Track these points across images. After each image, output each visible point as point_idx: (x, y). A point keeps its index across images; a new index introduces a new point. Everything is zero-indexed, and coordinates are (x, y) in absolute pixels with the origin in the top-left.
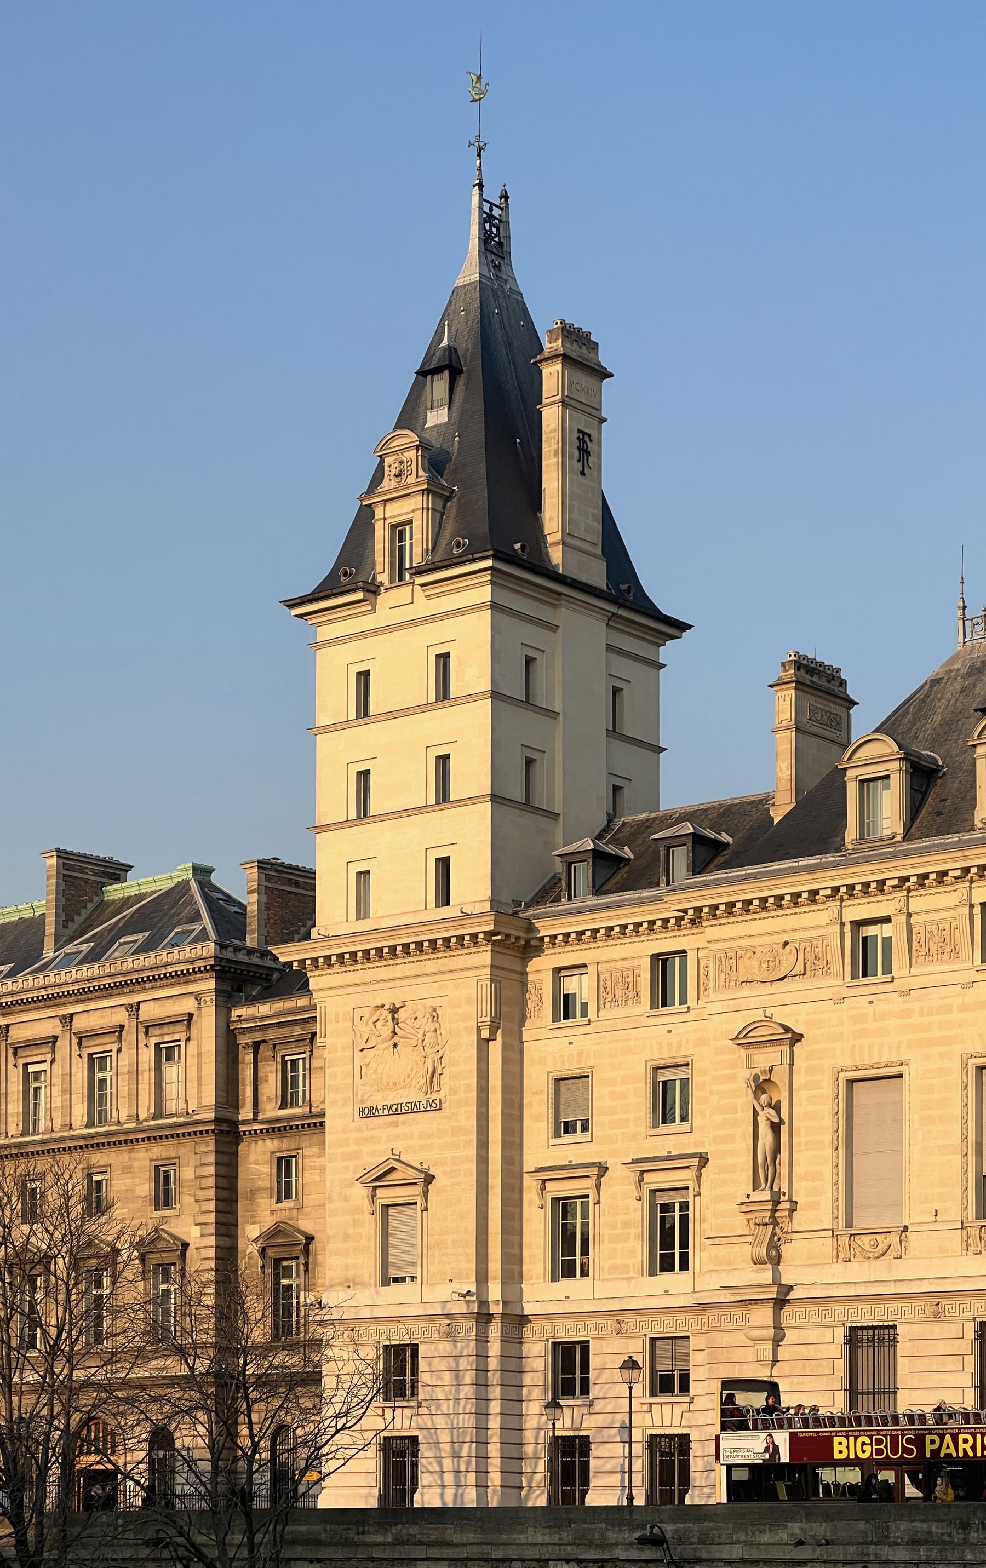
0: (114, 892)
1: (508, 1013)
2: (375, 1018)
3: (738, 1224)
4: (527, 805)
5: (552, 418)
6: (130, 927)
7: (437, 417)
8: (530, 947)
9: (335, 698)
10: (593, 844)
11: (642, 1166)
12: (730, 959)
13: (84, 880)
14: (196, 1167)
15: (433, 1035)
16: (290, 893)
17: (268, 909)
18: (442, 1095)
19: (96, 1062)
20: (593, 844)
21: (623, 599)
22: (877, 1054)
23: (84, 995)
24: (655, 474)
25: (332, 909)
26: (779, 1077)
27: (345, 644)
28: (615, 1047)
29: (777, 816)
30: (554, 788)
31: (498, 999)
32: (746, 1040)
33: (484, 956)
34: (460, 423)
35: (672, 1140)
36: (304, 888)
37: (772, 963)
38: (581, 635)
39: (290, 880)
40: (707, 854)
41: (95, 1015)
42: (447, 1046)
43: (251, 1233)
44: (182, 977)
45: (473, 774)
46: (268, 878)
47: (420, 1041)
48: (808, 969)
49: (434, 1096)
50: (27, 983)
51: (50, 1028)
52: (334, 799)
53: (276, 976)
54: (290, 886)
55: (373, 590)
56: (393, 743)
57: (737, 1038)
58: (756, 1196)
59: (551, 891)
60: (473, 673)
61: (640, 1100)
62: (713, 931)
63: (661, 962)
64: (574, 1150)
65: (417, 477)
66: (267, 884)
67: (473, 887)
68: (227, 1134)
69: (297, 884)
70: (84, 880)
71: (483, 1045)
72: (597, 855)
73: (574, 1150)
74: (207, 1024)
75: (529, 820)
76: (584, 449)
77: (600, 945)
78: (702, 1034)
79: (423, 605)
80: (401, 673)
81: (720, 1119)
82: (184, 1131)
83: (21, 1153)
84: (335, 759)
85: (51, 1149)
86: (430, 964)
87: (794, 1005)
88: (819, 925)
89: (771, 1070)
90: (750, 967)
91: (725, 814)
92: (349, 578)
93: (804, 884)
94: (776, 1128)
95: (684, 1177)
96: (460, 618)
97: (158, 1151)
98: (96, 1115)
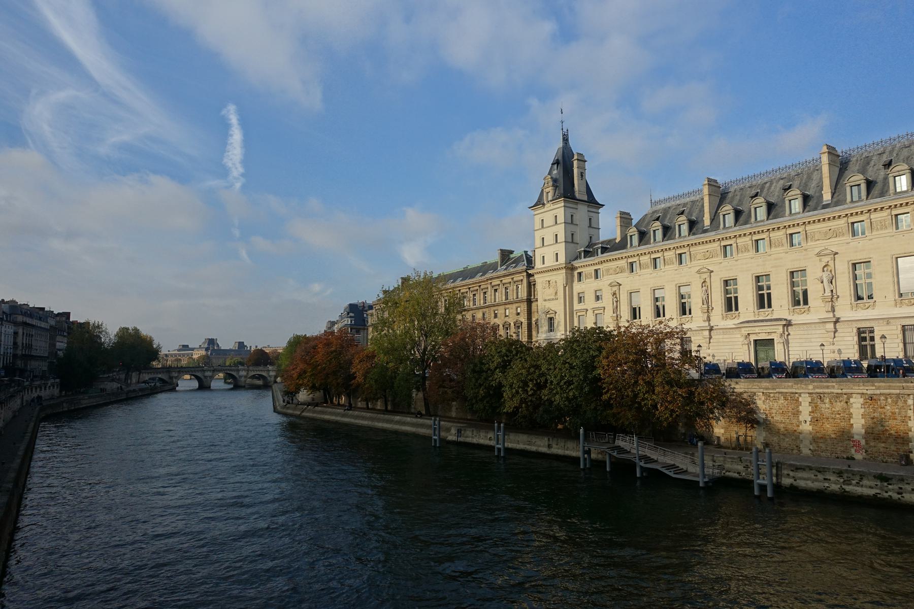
0: (512, 256)
1: (569, 282)
3: (611, 320)
4: (572, 242)
5: (576, 171)
6: (512, 263)
7: (555, 172)
8: (573, 269)
9: (538, 225)
10: (586, 248)
11: (594, 309)
12: (608, 270)
13: (506, 255)
14: (522, 309)
19: (506, 288)
20: (586, 248)
21: (592, 202)
22: (635, 287)
23: (504, 276)
24: (597, 178)
25: (538, 265)
26: (617, 292)
27: (540, 215)
28: (586, 287)
29: (617, 241)
30: (577, 238)
31: (567, 279)
32: (611, 285)
33: (564, 271)
34: (559, 173)
35: (599, 304)
37: (615, 270)
38: (582, 211)
40: (604, 250)
41: (507, 280)
43: (534, 319)
44: (520, 273)
45: (562, 238)
50: (495, 274)
51: (499, 282)
52: (538, 243)
55: (544, 204)
56: (546, 234)
59: (577, 257)
60: (561, 219)
61: (593, 297)
62: (604, 265)
63: (596, 271)
64: (581, 306)
65: (551, 184)
67: (562, 259)
68: (529, 302)
70: (506, 255)
71: (565, 287)
72: (585, 251)
73: (581, 306)
74: (525, 281)
75: (572, 245)
76: (582, 175)
77: (586, 266)
78: (603, 284)
79: (553, 207)
80: (549, 219)
81: (607, 301)
82: (521, 301)
83: (494, 306)
84: (538, 235)
85: (498, 305)
86: (555, 273)
87: (620, 278)
88: (623, 263)
90: (611, 271)
91: (609, 242)
92: (540, 203)
93: (620, 256)
95: (601, 311)
96: (557, 210)
97: (517, 305)
98: (507, 299)
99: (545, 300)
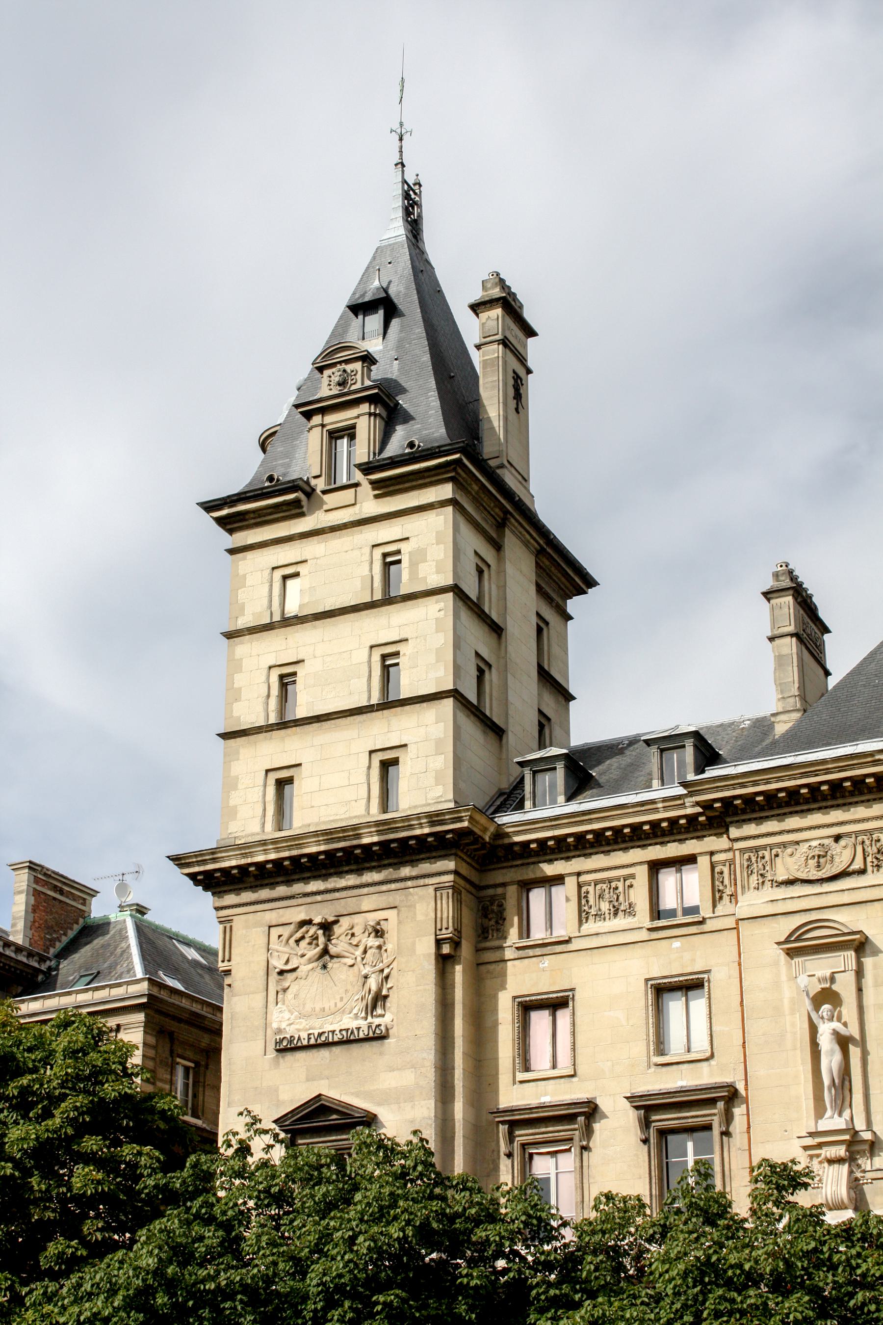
2: (298, 935)
15: (377, 951)
16: (55, 899)
17: (34, 911)
18: (387, 1020)
36: (67, 897)
39: (56, 886)
42: (394, 965)
46: (37, 880)
47: (359, 959)
48: (869, 864)
49: (377, 1021)
53: (40, 978)
54: (55, 892)
57: (787, 941)
58: (825, 1125)
66: (35, 886)
69: (61, 892)
71: (444, 962)
79: (370, 506)
89: (832, 979)
94: (843, 1042)
99: (287, 1048)
